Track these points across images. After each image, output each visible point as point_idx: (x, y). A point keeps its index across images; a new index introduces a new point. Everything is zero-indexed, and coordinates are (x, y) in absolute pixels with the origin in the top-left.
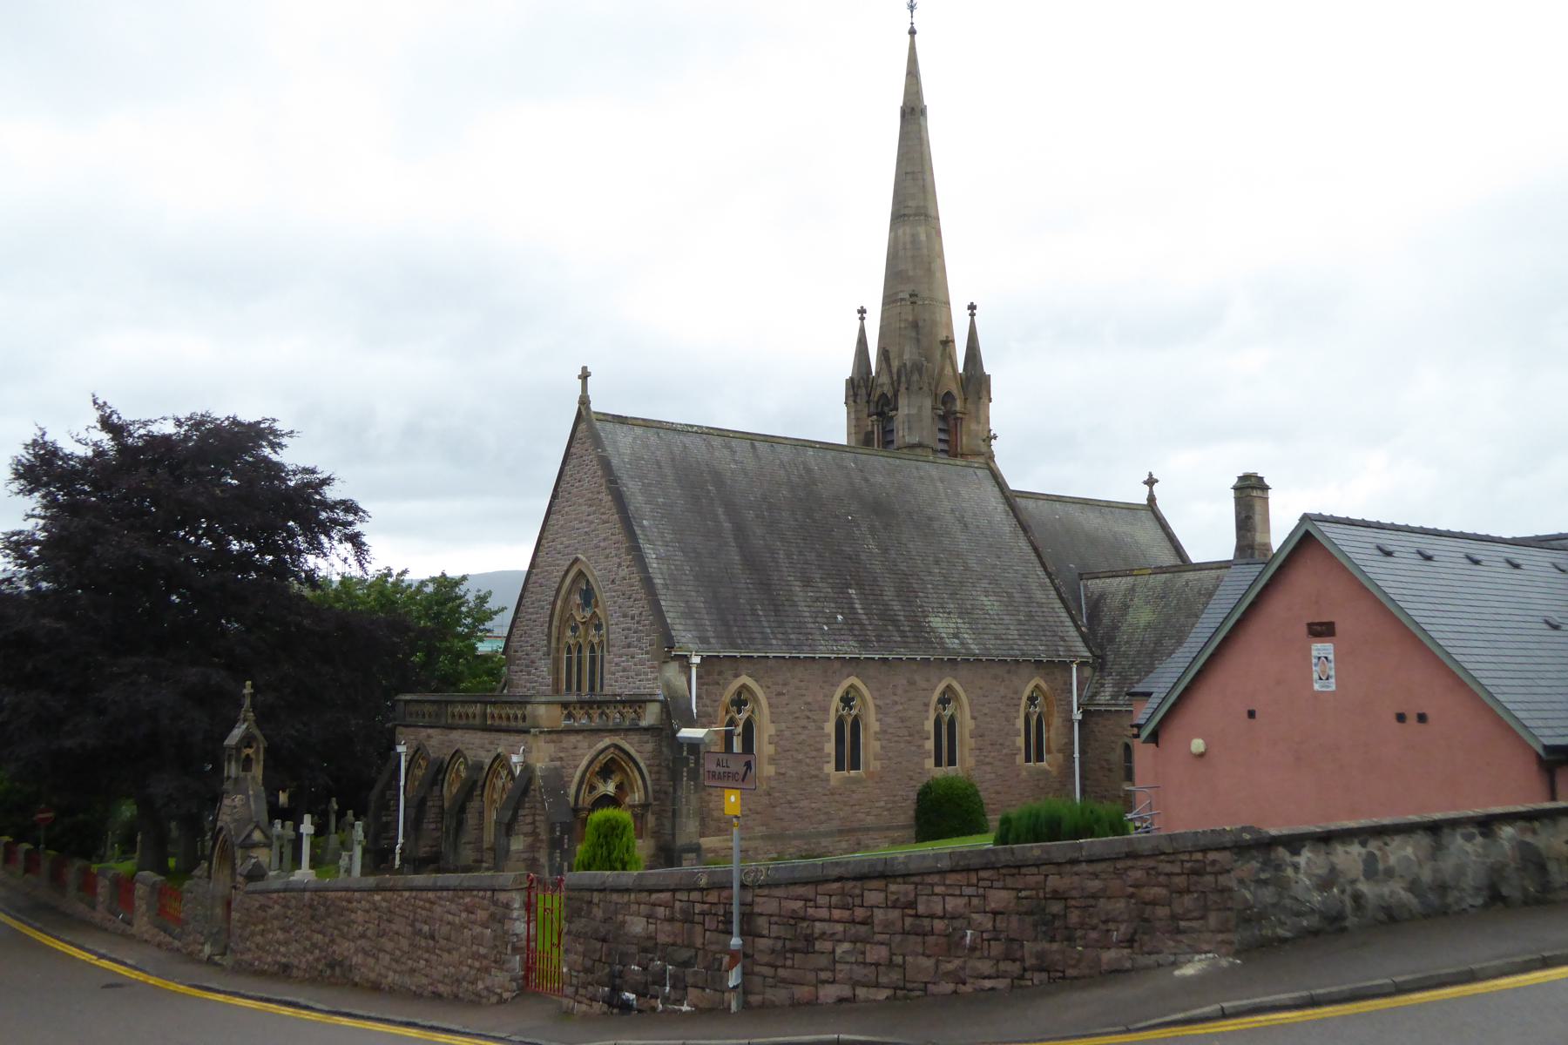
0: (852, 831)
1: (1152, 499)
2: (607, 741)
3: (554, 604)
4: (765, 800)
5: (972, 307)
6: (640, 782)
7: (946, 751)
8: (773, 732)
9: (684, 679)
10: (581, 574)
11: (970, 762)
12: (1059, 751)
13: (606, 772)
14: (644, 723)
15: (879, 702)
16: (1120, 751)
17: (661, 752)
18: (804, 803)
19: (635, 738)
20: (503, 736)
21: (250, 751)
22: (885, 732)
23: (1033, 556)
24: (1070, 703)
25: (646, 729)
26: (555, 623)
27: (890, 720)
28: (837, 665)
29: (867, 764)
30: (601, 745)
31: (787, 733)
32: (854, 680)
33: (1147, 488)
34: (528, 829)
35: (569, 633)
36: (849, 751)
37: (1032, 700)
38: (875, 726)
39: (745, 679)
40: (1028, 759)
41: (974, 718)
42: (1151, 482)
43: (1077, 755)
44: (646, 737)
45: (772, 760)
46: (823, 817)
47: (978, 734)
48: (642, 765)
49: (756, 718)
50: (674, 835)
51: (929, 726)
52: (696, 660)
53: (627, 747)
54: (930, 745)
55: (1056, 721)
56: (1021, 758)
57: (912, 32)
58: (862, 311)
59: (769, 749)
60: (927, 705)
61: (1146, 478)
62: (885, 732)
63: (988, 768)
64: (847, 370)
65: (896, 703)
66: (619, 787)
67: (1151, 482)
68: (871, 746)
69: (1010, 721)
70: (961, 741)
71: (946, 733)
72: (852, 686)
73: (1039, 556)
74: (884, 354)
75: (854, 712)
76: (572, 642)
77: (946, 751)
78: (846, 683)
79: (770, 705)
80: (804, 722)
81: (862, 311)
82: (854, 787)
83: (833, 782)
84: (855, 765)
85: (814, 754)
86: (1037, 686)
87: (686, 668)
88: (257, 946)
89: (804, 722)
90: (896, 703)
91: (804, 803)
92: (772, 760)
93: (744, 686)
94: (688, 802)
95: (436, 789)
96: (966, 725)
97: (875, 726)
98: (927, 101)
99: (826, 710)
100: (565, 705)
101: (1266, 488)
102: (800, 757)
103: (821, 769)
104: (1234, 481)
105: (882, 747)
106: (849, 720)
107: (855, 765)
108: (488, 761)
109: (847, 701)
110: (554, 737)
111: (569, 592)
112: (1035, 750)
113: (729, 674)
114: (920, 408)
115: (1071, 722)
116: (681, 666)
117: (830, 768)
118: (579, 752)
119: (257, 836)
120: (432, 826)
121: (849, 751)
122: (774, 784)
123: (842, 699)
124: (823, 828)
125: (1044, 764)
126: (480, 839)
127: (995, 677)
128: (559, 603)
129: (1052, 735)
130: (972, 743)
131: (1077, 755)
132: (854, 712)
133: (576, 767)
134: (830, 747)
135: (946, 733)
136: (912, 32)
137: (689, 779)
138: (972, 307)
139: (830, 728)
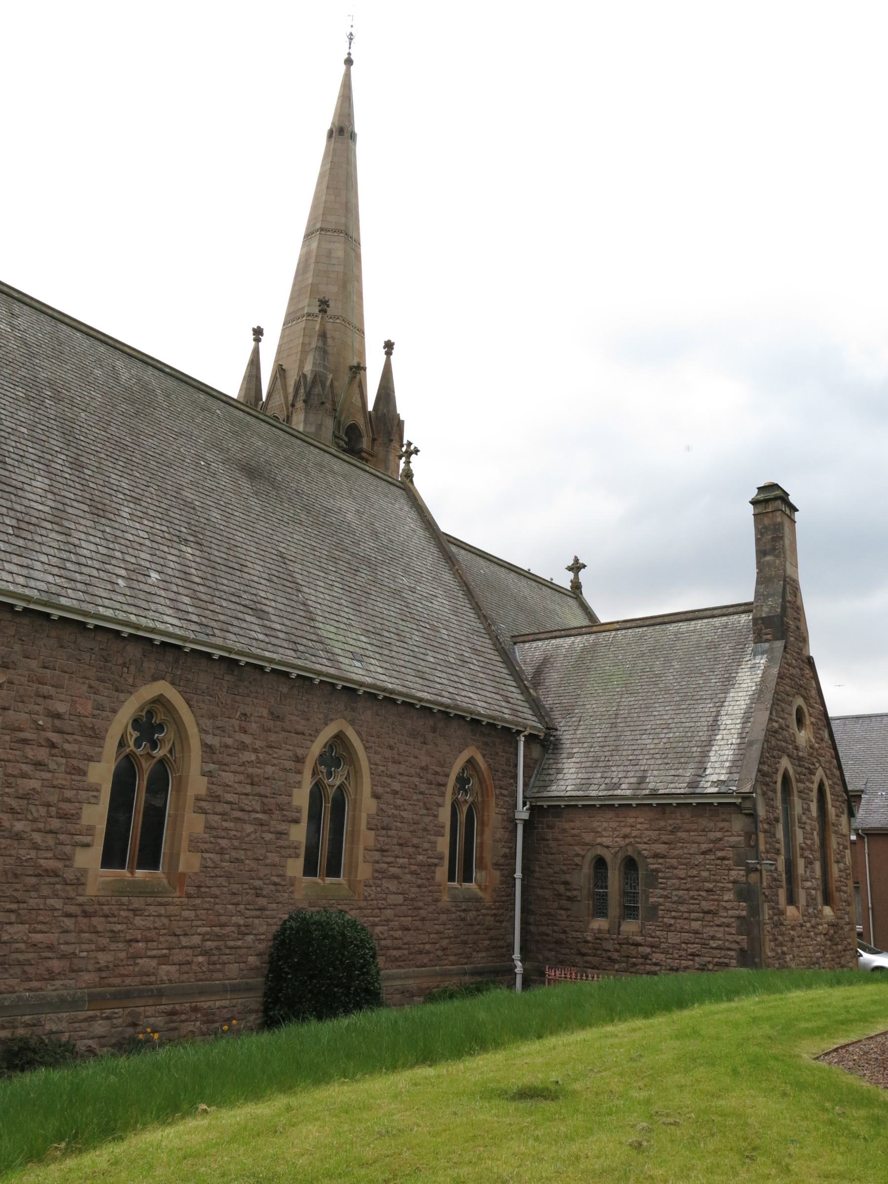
0: (125, 995)
1: (577, 586)
5: (389, 346)
7: (325, 858)
11: (364, 871)
12: (496, 865)
16: (587, 869)
22: (215, 798)
27: (228, 777)
28: (133, 651)
29: (174, 858)
32: (163, 688)
33: (571, 575)
36: (137, 834)
37: (462, 781)
40: (451, 878)
41: (376, 796)
43: (518, 874)
47: (379, 827)
51: (301, 799)
54: (299, 833)
56: (441, 873)
57: (349, 62)
58: (258, 333)
61: (570, 562)
62: (217, 799)
63: (392, 886)
65: (243, 747)
67: (576, 567)
69: (431, 810)
70: (354, 834)
71: (330, 812)
72: (160, 700)
75: (159, 753)
77: (325, 858)
78: (149, 692)
80: (42, 754)
81: (258, 333)
82: (137, 903)
83: (91, 889)
84: (150, 857)
85: (55, 824)
86: (471, 762)
89: (42, 754)
90: (243, 747)
96: (365, 805)
97: (197, 785)
98: (358, 129)
99: (96, 736)
103: (67, 859)
104: (753, 494)
105: (209, 827)
106: (147, 766)
107: (150, 857)
109: (148, 726)
112: (463, 865)
114: (320, 427)
115: (513, 821)
117: (89, 858)
121: (137, 834)
123: (136, 723)
124: (51, 990)
125: (473, 885)
127: (414, 734)
129: (489, 838)
130: (367, 837)
131: (518, 874)
132: (159, 753)
134: (96, 815)
135: (330, 812)
136: (349, 62)
138: (389, 346)
139: (102, 773)
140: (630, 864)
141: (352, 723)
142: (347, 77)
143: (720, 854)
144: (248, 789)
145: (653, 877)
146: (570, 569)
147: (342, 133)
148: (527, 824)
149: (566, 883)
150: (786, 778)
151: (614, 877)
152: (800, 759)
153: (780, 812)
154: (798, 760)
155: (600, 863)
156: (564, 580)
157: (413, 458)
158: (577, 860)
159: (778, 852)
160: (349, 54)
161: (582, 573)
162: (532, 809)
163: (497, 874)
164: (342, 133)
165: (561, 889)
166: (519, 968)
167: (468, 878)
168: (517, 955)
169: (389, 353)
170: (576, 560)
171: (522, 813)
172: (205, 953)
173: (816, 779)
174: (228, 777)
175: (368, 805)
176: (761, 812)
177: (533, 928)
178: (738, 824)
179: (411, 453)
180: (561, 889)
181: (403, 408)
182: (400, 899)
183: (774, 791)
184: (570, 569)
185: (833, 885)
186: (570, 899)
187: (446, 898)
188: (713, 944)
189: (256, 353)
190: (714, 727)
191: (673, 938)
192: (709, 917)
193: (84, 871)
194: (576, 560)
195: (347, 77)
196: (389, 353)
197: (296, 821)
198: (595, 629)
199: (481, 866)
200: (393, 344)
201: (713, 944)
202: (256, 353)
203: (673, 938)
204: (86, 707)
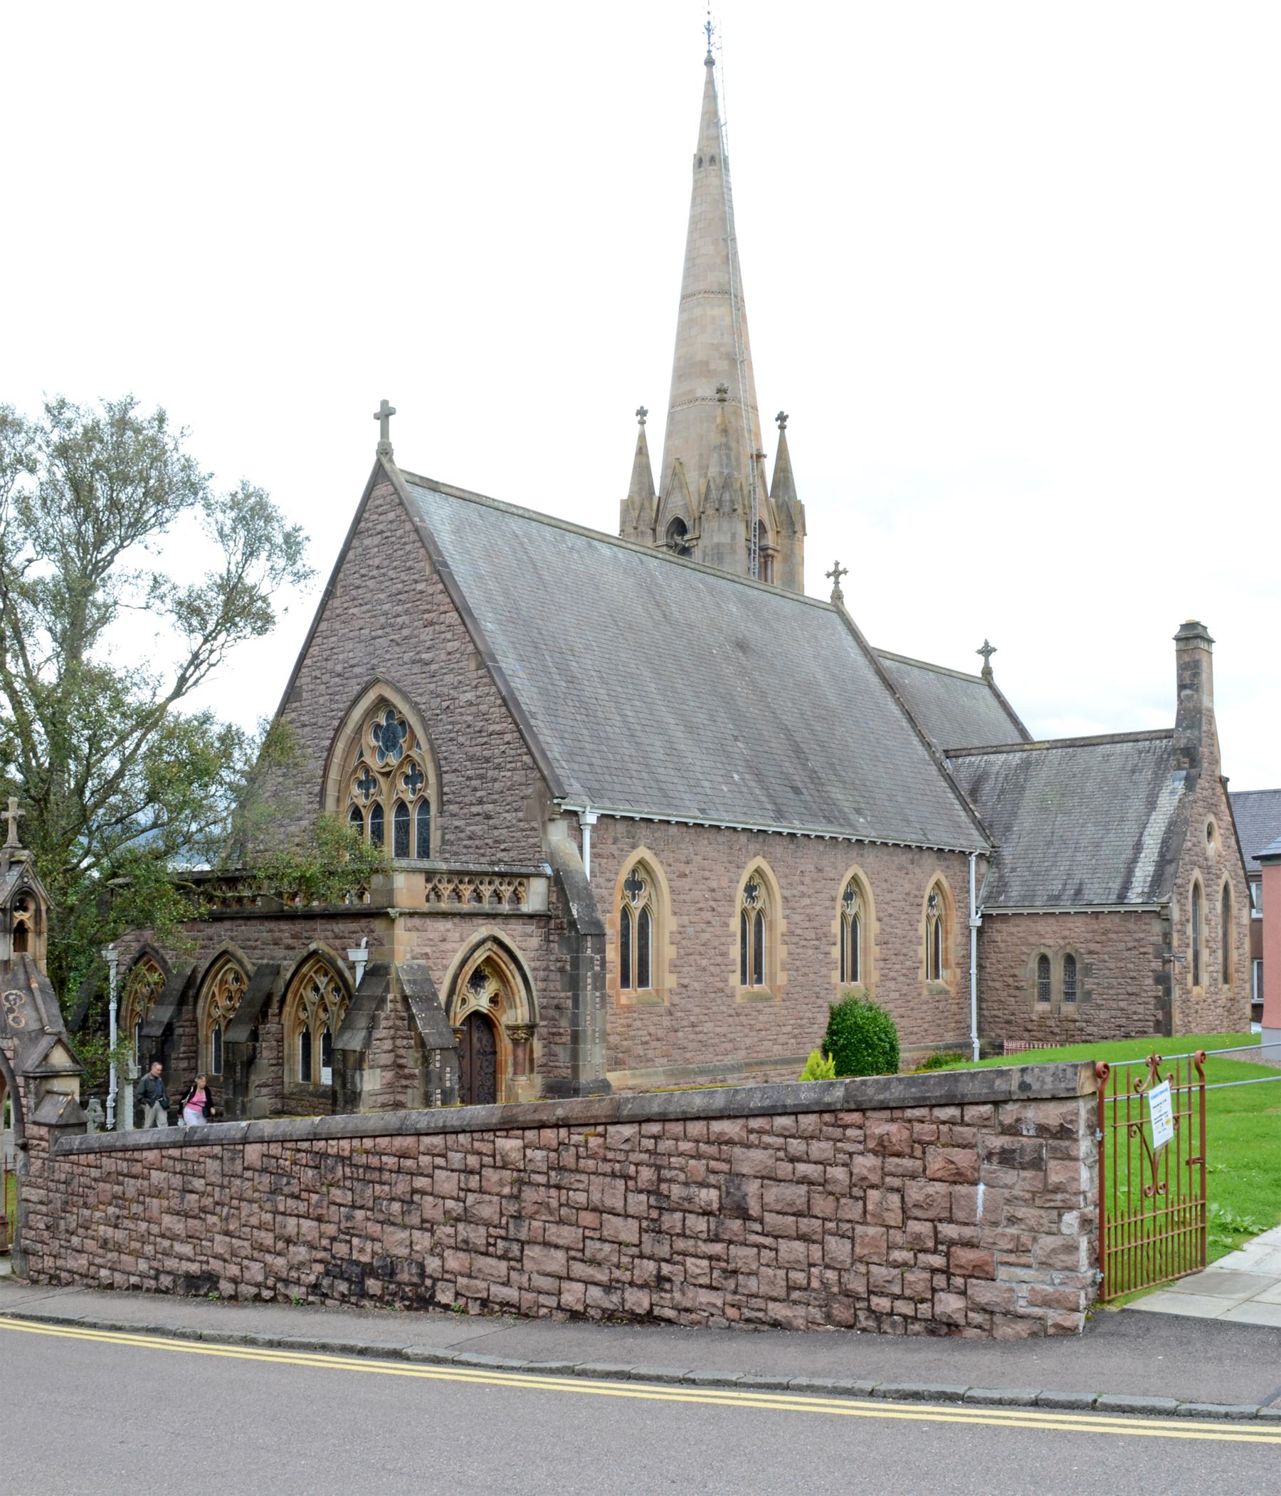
1: (987, 672)
2: (484, 930)
3: (331, 749)
4: (666, 1021)
5: (782, 418)
6: (523, 992)
8: (674, 928)
9: (574, 846)
10: (382, 702)
11: (875, 977)
13: (478, 979)
14: (526, 908)
15: (787, 893)
16: (1034, 964)
17: (549, 951)
18: (709, 1026)
19: (517, 927)
20: (318, 925)
21: (19, 916)
23: (905, 723)
24: (968, 907)
25: (531, 916)
26: (334, 775)
27: (797, 918)
28: (743, 838)
29: (772, 976)
30: (475, 938)
31: (690, 930)
32: (759, 862)
33: (981, 658)
34: (387, 1059)
35: (356, 790)
38: (782, 925)
39: (642, 852)
41: (879, 920)
42: (987, 651)
44: (531, 928)
45: (675, 967)
46: (729, 1046)
48: (526, 967)
49: (654, 907)
50: (575, 1069)
51: (836, 927)
52: (591, 819)
53: (507, 940)
55: (955, 927)
58: (642, 412)
59: (670, 952)
60: (833, 899)
61: (981, 646)
62: (792, 933)
63: (892, 985)
64: (623, 489)
65: (803, 895)
66: (494, 1000)
67: (987, 651)
68: (777, 952)
69: (912, 925)
70: (866, 949)
73: (911, 720)
74: (674, 470)
75: (758, 905)
76: (361, 801)
79: (672, 890)
81: (642, 412)
82: (760, 1006)
83: (738, 999)
85: (719, 959)
87: (578, 830)
88: (104, 1244)
89: (708, 916)
90: (803, 895)
91: (709, 1026)
92: (675, 967)
93: (642, 863)
94: (594, 1019)
95: (187, 1008)
96: (871, 928)
97: (782, 925)
99: (731, 900)
100: (430, 875)
101: (1210, 641)
102: (705, 963)
106: (753, 915)
108: (289, 966)
110: (417, 921)
111: (359, 730)
113: (624, 843)
114: (734, 536)
115: (968, 928)
116: (570, 827)
117: (735, 979)
118: (448, 946)
119: (60, 1058)
120: (184, 1064)
122: (676, 999)
124: (729, 1060)
125: (940, 981)
126: (279, 1080)
127: (900, 868)
128: (340, 746)
129: (952, 944)
130: (875, 951)
131: (974, 971)
133: (446, 968)
134: (735, 952)
137: (595, 988)
138: (782, 418)
139: (735, 924)
140: (1070, 960)
141: (862, 866)
142: (710, 83)
143: (1142, 950)
144: (807, 924)
145: (1088, 969)
146: (980, 652)
147: (710, 161)
148: (980, 931)
149: (1014, 976)
150: (1196, 887)
151: (1057, 972)
152: (1209, 867)
153: (1190, 915)
154: (1207, 869)
155: (1044, 960)
156: (974, 667)
157: (842, 577)
158: (1024, 957)
159: (1187, 945)
160: (709, 52)
161: (992, 658)
162: (983, 916)
163: (958, 971)
164: (710, 161)
165: (1010, 980)
166: (977, 1044)
167: (937, 976)
168: (974, 1034)
169: (782, 428)
170: (987, 643)
171: (976, 921)
172: (795, 1037)
173: (1222, 882)
174: (797, 918)
175: (875, 927)
176: (1176, 915)
177: (985, 1013)
178: (1157, 927)
179: (840, 573)
180: (1010, 980)
181: (804, 490)
182: (896, 995)
183: (1186, 898)
184: (980, 652)
185: (1232, 969)
186: (1017, 988)
187: (925, 992)
188: (1135, 1017)
189: (642, 437)
190: (1138, 847)
191: (1103, 1015)
192: (1133, 997)
193: (734, 988)
194: (987, 643)
195: (710, 83)
196: (782, 428)
197: (834, 944)
198: (1027, 747)
199: (946, 966)
200: (787, 417)
201: (1135, 1017)
202: (642, 437)
203: (1103, 1015)
204: (725, 883)
